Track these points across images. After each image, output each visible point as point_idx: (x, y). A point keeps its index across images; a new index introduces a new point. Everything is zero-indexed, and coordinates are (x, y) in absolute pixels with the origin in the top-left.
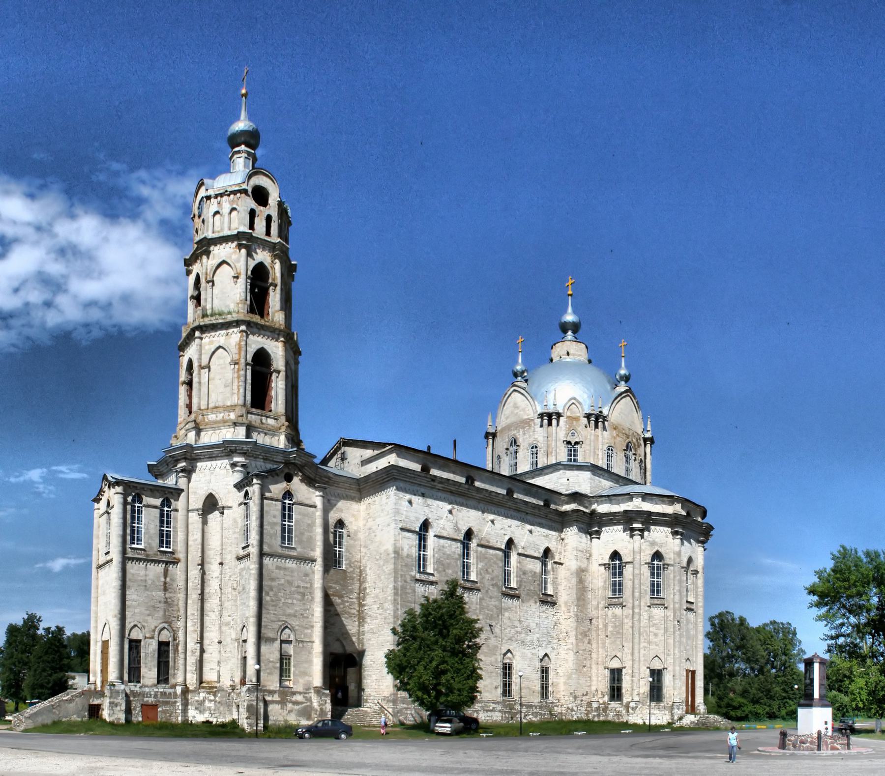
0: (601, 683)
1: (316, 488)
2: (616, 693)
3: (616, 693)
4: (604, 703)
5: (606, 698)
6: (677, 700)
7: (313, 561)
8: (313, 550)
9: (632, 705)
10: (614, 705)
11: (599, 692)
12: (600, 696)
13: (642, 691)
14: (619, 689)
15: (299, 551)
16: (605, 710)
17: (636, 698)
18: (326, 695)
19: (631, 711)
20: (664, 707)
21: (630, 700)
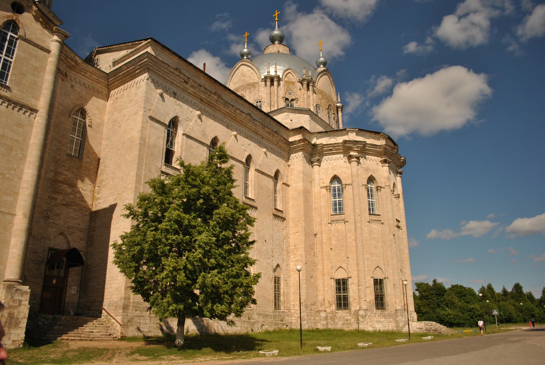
0: (329, 293)
1: (53, 32)
2: (343, 302)
3: (343, 302)
4: (332, 312)
5: (334, 307)
6: (398, 307)
7: (34, 111)
8: (37, 98)
9: (361, 313)
10: (342, 313)
11: (326, 302)
12: (327, 305)
13: (368, 300)
14: (346, 298)
15: (15, 94)
16: (333, 319)
17: (365, 307)
18: (23, 293)
19: (360, 318)
20: (389, 315)
21: (358, 308)
